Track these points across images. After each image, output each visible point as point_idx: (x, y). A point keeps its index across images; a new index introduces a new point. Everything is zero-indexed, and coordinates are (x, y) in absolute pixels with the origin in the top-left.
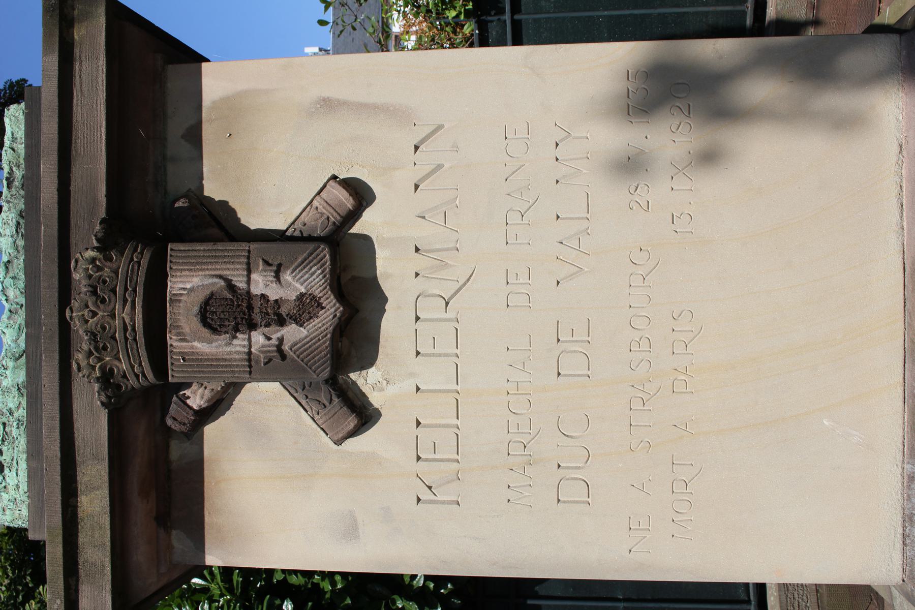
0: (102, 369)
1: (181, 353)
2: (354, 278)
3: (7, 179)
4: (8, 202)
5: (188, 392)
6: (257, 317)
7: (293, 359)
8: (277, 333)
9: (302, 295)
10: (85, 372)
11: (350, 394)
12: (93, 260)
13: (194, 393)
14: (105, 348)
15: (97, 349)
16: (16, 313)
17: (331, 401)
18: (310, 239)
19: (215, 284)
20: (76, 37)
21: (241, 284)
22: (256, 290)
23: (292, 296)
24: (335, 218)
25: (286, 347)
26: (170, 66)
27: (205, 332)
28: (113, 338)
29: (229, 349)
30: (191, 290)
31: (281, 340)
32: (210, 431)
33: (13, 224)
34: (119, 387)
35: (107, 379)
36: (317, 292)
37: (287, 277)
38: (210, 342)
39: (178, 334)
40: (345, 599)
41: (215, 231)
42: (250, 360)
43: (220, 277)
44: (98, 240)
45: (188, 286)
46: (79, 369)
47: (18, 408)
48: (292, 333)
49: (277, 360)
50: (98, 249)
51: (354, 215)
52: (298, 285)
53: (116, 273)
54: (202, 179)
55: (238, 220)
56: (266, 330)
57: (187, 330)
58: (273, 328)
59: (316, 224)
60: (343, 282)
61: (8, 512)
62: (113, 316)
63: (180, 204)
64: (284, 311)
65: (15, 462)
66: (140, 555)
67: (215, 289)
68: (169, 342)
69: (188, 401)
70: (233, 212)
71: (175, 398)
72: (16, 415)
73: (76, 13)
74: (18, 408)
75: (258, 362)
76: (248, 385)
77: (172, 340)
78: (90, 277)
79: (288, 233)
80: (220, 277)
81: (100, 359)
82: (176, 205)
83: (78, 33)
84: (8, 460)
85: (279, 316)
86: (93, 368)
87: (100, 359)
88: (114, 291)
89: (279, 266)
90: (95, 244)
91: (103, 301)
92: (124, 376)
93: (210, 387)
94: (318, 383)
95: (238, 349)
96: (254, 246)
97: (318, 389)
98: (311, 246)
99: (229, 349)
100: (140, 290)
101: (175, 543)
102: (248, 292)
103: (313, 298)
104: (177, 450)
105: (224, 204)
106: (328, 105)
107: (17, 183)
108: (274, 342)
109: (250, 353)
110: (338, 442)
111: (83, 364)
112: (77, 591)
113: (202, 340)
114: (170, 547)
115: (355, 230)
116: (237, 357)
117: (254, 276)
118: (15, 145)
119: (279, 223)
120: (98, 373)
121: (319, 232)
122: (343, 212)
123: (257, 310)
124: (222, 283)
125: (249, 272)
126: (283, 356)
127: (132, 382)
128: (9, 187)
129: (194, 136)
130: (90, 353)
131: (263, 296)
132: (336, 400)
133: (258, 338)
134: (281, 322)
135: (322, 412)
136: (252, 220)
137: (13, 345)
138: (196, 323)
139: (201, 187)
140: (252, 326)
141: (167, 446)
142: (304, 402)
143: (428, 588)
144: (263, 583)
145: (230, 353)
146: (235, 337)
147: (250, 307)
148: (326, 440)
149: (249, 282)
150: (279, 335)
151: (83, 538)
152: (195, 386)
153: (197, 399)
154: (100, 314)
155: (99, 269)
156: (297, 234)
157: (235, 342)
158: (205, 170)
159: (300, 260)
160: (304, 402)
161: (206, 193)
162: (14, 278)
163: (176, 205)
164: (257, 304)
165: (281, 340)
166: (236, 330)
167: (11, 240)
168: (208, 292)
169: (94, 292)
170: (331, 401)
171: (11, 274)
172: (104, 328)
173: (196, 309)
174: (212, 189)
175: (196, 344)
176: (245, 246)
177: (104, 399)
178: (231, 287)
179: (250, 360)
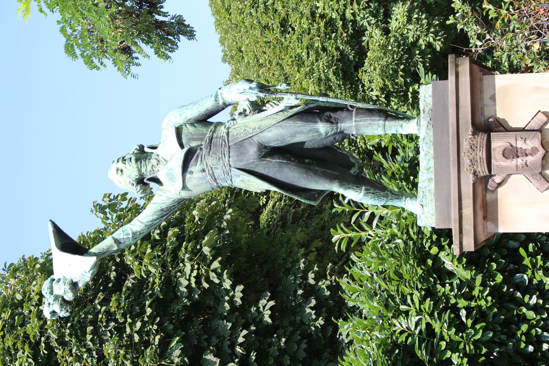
0: (474, 170)
1: (496, 165)
2: (546, 142)
3: (423, 111)
4: (424, 118)
5: (495, 178)
6: (519, 154)
7: (530, 167)
8: (525, 159)
9: (533, 147)
10: (469, 171)
11: (546, 177)
12: (471, 138)
13: (497, 178)
14: (474, 164)
15: (472, 164)
16: (427, 155)
17: (541, 179)
18: (534, 130)
19: (506, 145)
20: (459, 70)
21: (514, 145)
22: (519, 146)
23: (530, 148)
24: (541, 124)
25: (528, 163)
26: (484, 76)
27: (504, 159)
28: (477, 161)
29: (511, 164)
30: (499, 147)
31: (526, 161)
32: (500, 190)
33: (426, 125)
34: (477, 176)
35: (475, 173)
36: (537, 146)
37: (528, 142)
38: (505, 162)
39: (495, 160)
40: (494, 309)
41: (502, 128)
42: (517, 167)
43: (508, 142)
44: (472, 132)
45: (498, 145)
46: (467, 170)
47: (428, 186)
48: (530, 159)
49: (525, 167)
50: (472, 135)
51: (546, 123)
52: (531, 144)
53: (477, 142)
54: (496, 111)
55: (508, 124)
56: (521, 158)
57: (498, 158)
58: (524, 157)
59: (534, 125)
60: (543, 143)
61: (423, 221)
62: (477, 155)
63: (491, 120)
64: (527, 152)
65: (427, 204)
66: (480, 228)
67: (507, 146)
68: (492, 162)
69: (495, 181)
70: (507, 122)
71: (490, 179)
72: (427, 188)
73: (459, 63)
74: (428, 186)
75: (519, 168)
76: (512, 176)
77: (493, 161)
78: (470, 143)
79: (526, 128)
80: (508, 142)
81: (473, 167)
82: (490, 120)
83: (460, 69)
84: (425, 203)
85: (526, 154)
86: (471, 170)
87: (473, 167)
88: (477, 147)
89: (525, 139)
90: (471, 133)
91: (474, 150)
92: (479, 173)
93: (502, 176)
94: (536, 174)
95: (514, 164)
96: (517, 133)
97: (537, 175)
98: (535, 133)
99: (511, 164)
100: (484, 147)
101: (488, 226)
102: (516, 147)
103: (536, 148)
104: (489, 196)
105: (504, 119)
106: (537, 89)
107: (426, 112)
108: (525, 161)
109: (517, 165)
110: (542, 192)
111: (468, 169)
112: (462, 238)
113: (504, 161)
114: (487, 227)
115: (546, 127)
116: (513, 166)
117: (518, 142)
118: (425, 99)
119: (521, 125)
120: (472, 172)
121: (536, 128)
122: (544, 122)
123: (519, 152)
124: (509, 144)
125: (516, 140)
126: (527, 166)
127: (482, 175)
129: (493, 98)
130: (470, 166)
131: (521, 148)
132: (542, 179)
133: (519, 160)
134: (527, 155)
135: (538, 182)
136: (513, 124)
137: (426, 165)
138: (501, 156)
139: (496, 114)
140: (518, 157)
141: (486, 195)
142: (532, 180)
143: (539, 303)
144: (444, 305)
145: (511, 165)
146: (513, 160)
147: (517, 151)
148: (538, 191)
149: (516, 144)
150: (526, 159)
151: (464, 223)
152: (497, 176)
153: (498, 179)
154: (473, 154)
155: (473, 141)
156: (529, 129)
157: (513, 162)
158: (497, 109)
159: (531, 137)
160: (532, 180)
161: (498, 116)
162: (426, 143)
163: (490, 120)
164: (519, 150)
165: (526, 161)
166: (513, 158)
167: (425, 131)
168: (504, 147)
169: (471, 148)
170: (541, 179)
171: (425, 142)
172: (474, 158)
173: (501, 152)
174: (500, 115)
175: (501, 162)
176: (514, 133)
177: (473, 179)
178: (511, 146)
179: (517, 167)
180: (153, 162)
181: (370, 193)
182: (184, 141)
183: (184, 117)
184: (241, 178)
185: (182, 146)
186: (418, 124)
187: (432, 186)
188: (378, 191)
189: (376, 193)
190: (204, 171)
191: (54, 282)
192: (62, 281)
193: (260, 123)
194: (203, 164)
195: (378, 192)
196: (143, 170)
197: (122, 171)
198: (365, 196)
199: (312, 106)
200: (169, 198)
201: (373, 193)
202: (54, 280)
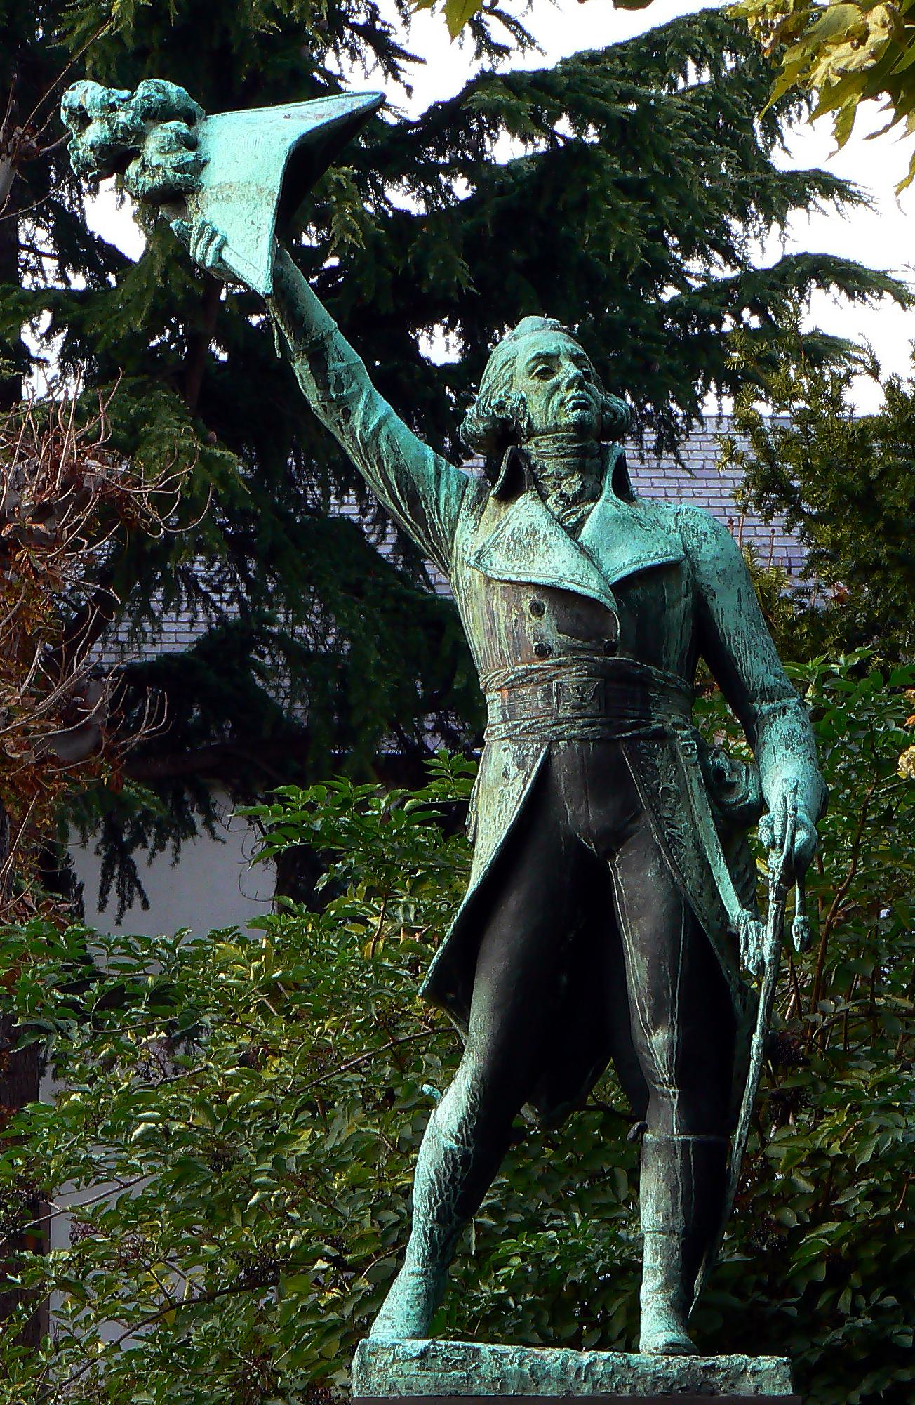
3: (713, 1365)
4: (689, 1367)
128: (706, 1369)
180: (572, 485)
181: (455, 1169)
182: (637, 593)
183: (715, 584)
184: (514, 770)
185: (622, 588)
186: (672, 1349)
187: (479, 1389)
188: (460, 1192)
189: (455, 1187)
190: (543, 652)
191: (183, 127)
192: (190, 156)
193: (688, 842)
194: (564, 654)
195: (456, 1193)
196: (546, 445)
197: (546, 374)
198: (446, 1154)
199: (738, 1004)
200: (454, 522)
201: (452, 1179)
202: (190, 119)
